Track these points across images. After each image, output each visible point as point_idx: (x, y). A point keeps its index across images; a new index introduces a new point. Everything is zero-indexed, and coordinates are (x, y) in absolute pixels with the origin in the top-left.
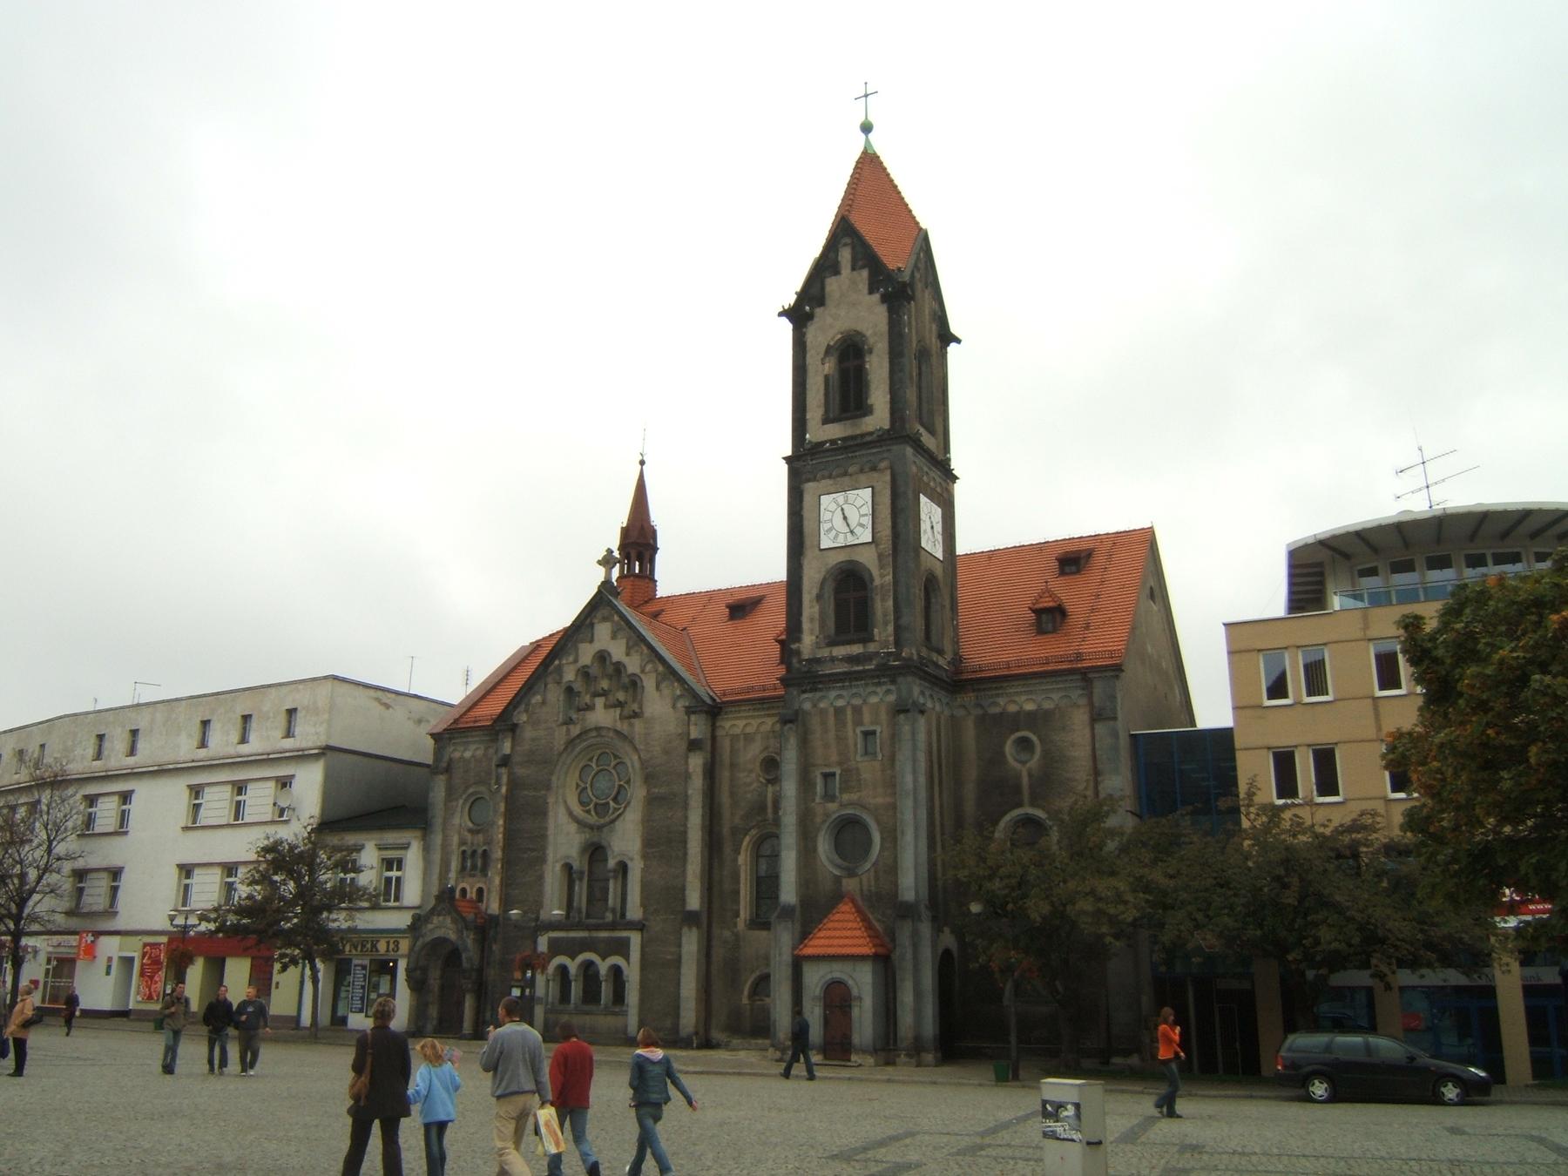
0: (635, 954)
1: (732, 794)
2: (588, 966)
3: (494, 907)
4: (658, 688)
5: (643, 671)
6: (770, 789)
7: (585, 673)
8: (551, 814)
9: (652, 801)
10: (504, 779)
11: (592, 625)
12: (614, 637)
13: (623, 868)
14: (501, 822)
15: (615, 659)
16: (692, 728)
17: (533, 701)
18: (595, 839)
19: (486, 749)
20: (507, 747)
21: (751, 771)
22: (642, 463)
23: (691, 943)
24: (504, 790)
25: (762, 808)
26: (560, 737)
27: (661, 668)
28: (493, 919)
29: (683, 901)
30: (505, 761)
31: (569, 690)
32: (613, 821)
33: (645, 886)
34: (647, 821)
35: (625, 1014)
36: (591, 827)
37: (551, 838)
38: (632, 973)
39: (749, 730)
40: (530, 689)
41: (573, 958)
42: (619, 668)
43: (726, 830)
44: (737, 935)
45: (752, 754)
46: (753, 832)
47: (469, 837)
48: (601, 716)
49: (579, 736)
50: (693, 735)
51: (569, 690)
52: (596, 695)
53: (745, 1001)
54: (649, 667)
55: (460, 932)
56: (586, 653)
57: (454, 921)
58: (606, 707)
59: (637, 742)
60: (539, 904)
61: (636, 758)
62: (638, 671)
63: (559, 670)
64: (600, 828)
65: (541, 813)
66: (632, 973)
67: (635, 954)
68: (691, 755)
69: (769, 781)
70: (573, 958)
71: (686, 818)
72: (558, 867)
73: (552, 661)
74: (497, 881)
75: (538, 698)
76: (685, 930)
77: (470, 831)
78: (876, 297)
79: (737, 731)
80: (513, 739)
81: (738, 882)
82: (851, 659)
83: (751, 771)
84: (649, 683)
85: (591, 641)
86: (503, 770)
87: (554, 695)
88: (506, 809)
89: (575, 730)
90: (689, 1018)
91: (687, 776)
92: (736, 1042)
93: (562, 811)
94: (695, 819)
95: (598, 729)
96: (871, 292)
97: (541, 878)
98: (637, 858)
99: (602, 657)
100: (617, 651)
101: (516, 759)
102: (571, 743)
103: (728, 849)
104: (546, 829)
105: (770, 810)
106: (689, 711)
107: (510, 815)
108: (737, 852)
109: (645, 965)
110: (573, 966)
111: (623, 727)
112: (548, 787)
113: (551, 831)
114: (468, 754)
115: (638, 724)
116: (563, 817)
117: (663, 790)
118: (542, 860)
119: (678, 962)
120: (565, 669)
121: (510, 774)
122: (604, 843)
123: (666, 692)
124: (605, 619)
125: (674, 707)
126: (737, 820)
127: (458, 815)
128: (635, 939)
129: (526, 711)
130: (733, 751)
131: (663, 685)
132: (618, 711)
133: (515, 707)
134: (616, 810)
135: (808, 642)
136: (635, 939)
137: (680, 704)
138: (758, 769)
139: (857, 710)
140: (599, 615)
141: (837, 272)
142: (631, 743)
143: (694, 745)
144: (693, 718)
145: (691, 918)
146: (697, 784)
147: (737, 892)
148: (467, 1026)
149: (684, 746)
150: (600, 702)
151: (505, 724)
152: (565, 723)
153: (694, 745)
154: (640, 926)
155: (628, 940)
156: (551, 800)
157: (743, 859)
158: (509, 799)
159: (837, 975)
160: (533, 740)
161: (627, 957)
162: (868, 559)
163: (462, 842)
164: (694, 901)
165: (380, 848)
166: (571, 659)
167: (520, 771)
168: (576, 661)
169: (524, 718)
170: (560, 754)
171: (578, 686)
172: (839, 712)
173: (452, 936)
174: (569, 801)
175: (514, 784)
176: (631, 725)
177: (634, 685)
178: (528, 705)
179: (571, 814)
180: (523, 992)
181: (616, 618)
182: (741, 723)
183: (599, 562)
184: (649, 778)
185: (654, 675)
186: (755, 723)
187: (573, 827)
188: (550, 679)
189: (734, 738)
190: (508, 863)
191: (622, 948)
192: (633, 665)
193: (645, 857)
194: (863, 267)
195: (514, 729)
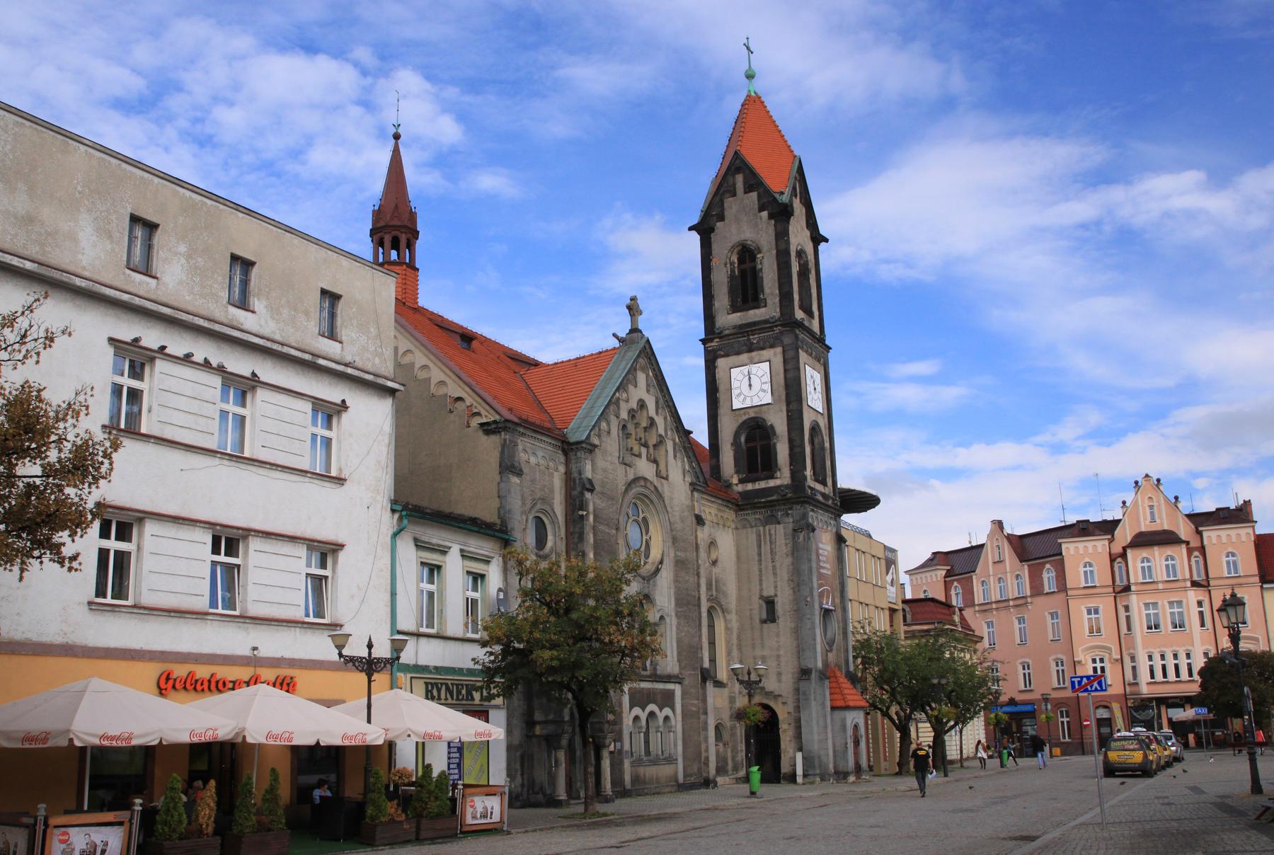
4: (675, 457)
6: (715, 570)
9: (680, 564)
14: (591, 556)
22: (397, 137)
26: (621, 477)
38: (677, 723)
48: (644, 468)
71: (699, 585)
82: (823, 495)
89: (631, 477)
95: (645, 479)
102: (630, 485)
114: (533, 460)
123: (679, 464)
124: (643, 369)
135: (809, 472)
137: (688, 479)
144: (696, 494)
150: (644, 450)
161: (673, 710)
162: (823, 423)
165: (465, 555)
166: (625, 395)
168: (627, 401)
184: (674, 540)
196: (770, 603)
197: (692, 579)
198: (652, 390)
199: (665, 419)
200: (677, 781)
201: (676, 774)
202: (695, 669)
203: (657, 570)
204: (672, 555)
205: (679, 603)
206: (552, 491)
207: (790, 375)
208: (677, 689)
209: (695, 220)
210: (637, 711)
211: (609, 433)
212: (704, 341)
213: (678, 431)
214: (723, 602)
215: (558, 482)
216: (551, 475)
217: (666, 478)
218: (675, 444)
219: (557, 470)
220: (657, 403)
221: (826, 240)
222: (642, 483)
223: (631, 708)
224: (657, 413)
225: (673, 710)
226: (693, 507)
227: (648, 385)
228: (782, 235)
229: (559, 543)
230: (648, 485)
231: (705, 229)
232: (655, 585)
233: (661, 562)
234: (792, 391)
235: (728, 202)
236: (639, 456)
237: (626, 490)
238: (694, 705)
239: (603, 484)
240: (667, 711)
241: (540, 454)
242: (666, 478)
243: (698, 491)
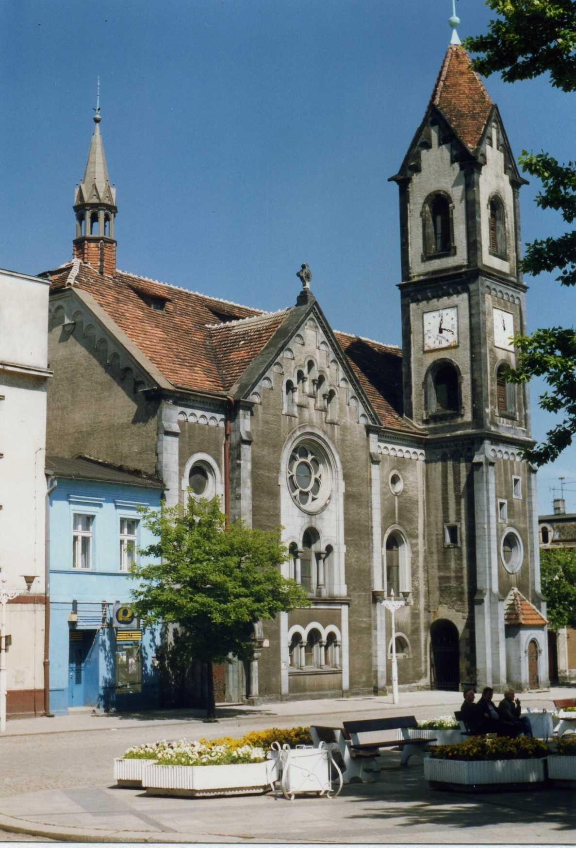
2: (314, 636)
13: (329, 549)
29: (370, 581)
33: (348, 567)
38: (343, 637)
41: (305, 627)
70: (305, 627)
78: (506, 178)
96: (505, 173)
105: (397, 516)
106: (369, 430)
109: (352, 632)
121: (253, 452)
122: (318, 528)
128: (345, 609)
134: (313, 499)
137: (363, 421)
139: (512, 463)
141: (491, 145)
144: (372, 435)
159: (534, 636)
161: (340, 628)
172: (505, 462)
184: (346, 477)
193: (346, 543)
194: (501, 151)
195: (250, 407)
196: (453, 531)
199: (337, 370)
201: (341, 682)
202: (365, 590)
205: (347, 532)
207: (474, 320)
208: (345, 609)
209: (395, 171)
210: (297, 628)
212: (400, 287)
221: (527, 183)
223: (291, 625)
225: (340, 628)
228: (470, 185)
231: (403, 181)
234: (477, 334)
235: (424, 153)
238: (365, 622)
240: (332, 628)
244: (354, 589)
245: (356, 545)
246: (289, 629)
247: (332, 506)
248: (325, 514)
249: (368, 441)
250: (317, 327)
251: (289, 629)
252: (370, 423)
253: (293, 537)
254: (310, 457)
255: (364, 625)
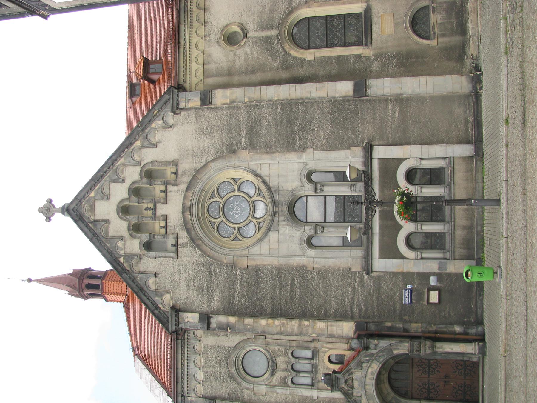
0: (395, 152)
1: (253, 72)
3: (347, 328)
4: (155, 146)
5: (139, 163)
7: (136, 228)
8: (259, 262)
9: (253, 146)
10: (222, 319)
11: (95, 221)
12: (107, 197)
14: (263, 322)
15: (126, 195)
16: (191, 105)
17: (153, 287)
18: (285, 209)
19: (195, 352)
20: (192, 318)
21: (235, 55)
23: (381, 87)
24: (232, 319)
25: (267, 40)
26: (189, 255)
27: (138, 143)
28: (358, 327)
29: (345, 100)
30: (206, 318)
31: (148, 246)
32: (269, 188)
33: (331, 147)
34: (269, 149)
35: (451, 160)
36: (274, 213)
37: (282, 261)
39: (201, 60)
40: (141, 289)
42: (135, 192)
43: (284, 75)
44: (378, 56)
45: (220, 55)
46: (287, 47)
47: (279, 374)
48: (172, 209)
49: (188, 231)
50: (199, 103)
51: (148, 246)
52: (154, 216)
53: (434, 43)
54: (136, 157)
55: (372, 358)
56: (119, 226)
57: (360, 365)
58: (165, 202)
59: (200, 165)
60: (347, 272)
61: (212, 165)
62: (138, 169)
63: (129, 257)
64: (275, 204)
65: (256, 274)
66: (412, 155)
67: (395, 152)
68: (214, 101)
69: (245, 36)
71: (270, 100)
72: (310, 252)
73: (119, 263)
74: (321, 325)
75: (151, 281)
76: (370, 92)
77: (272, 375)
79: (201, 70)
80: (185, 311)
81: (330, 58)
83: (235, 55)
84: (149, 156)
85: (108, 221)
86: (214, 322)
87: (150, 263)
88: (251, 315)
90: (456, 84)
91: (233, 105)
92: (472, 49)
93: (256, 250)
94: (270, 93)
95: (184, 210)
97: (322, 273)
98: (303, 155)
99: (124, 210)
100: (119, 192)
101: (204, 308)
102: (194, 241)
103: (301, 72)
104: (273, 267)
106: (176, 109)
107: (258, 313)
108: (303, 61)
110: (408, 227)
111: (185, 180)
112: (234, 266)
113: (275, 262)
115: (186, 166)
116: (263, 248)
117: (243, 133)
118: (304, 269)
119: (401, 101)
120: (128, 251)
121: (218, 313)
123: (160, 135)
124: (92, 208)
125: (172, 126)
126: (276, 64)
127: (256, 388)
129: (161, 296)
130: (219, 74)
131: (153, 140)
132: (170, 188)
133: (157, 307)
136: (381, 152)
137: (170, 118)
138: (233, 48)
140: (87, 214)
142: (199, 171)
143: (206, 100)
144: (183, 105)
145: (360, 89)
146: (238, 93)
147: (338, 58)
148: (470, 349)
149: (207, 114)
150: (161, 210)
151: (171, 321)
152: (177, 252)
153: (206, 100)
154: (368, 151)
155: (383, 162)
156: (245, 262)
157: (310, 55)
158: (241, 314)
160: (188, 286)
161: (401, 160)
163: (284, 383)
164: (345, 88)
166: (120, 244)
167: (216, 304)
168: (123, 238)
169: (167, 297)
170: (204, 253)
171: (145, 237)
173: (375, 367)
174: (249, 244)
175: (228, 311)
176: (184, 171)
177: (149, 175)
178: (156, 293)
179: (260, 240)
180: (434, 289)
181: (92, 195)
182: (195, 66)
183: (49, 219)
184: (232, 150)
185: (144, 151)
186: (195, 52)
187: (273, 236)
188: (136, 269)
189: (207, 75)
190: (304, 315)
191: (389, 167)
192: (132, 174)
193: (303, 149)
195: (176, 310)
197: (266, 113)
198: (106, 190)
199: (125, 165)
200: (471, 158)
201: (464, 158)
203: (264, 182)
204: (244, 154)
206: (218, 349)
208: (381, 152)
211: (156, 275)
213: (131, 144)
214: (282, 9)
215: (210, 340)
216: (206, 347)
217: (176, 164)
218: (142, 147)
219: (201, 341)
220: (114, 181)
222: (188, 213)
224: (123, 181)
225: (401, 160)
226: (196, 109)
227: (102, 199)
229: (259, 342)
230: (188, 203)
232: (278, 191)
233: (257, 175)
236: (165, 218)
237: (199, 247)
238: (393, 112)
239: (200, 290)
241: (192, 366)
242: (176, 164)
243: (178, 104)
244: (355, 131)
245: (304, 127)
246: (403, 257)
247: (264, 171)
248: (272, 183)
249: (189, 109)
250: (88, 201)
251: (403, 257)
252: (169, 105)
253: (301, 240)
254: (218, 199)
255: (397, 113)
